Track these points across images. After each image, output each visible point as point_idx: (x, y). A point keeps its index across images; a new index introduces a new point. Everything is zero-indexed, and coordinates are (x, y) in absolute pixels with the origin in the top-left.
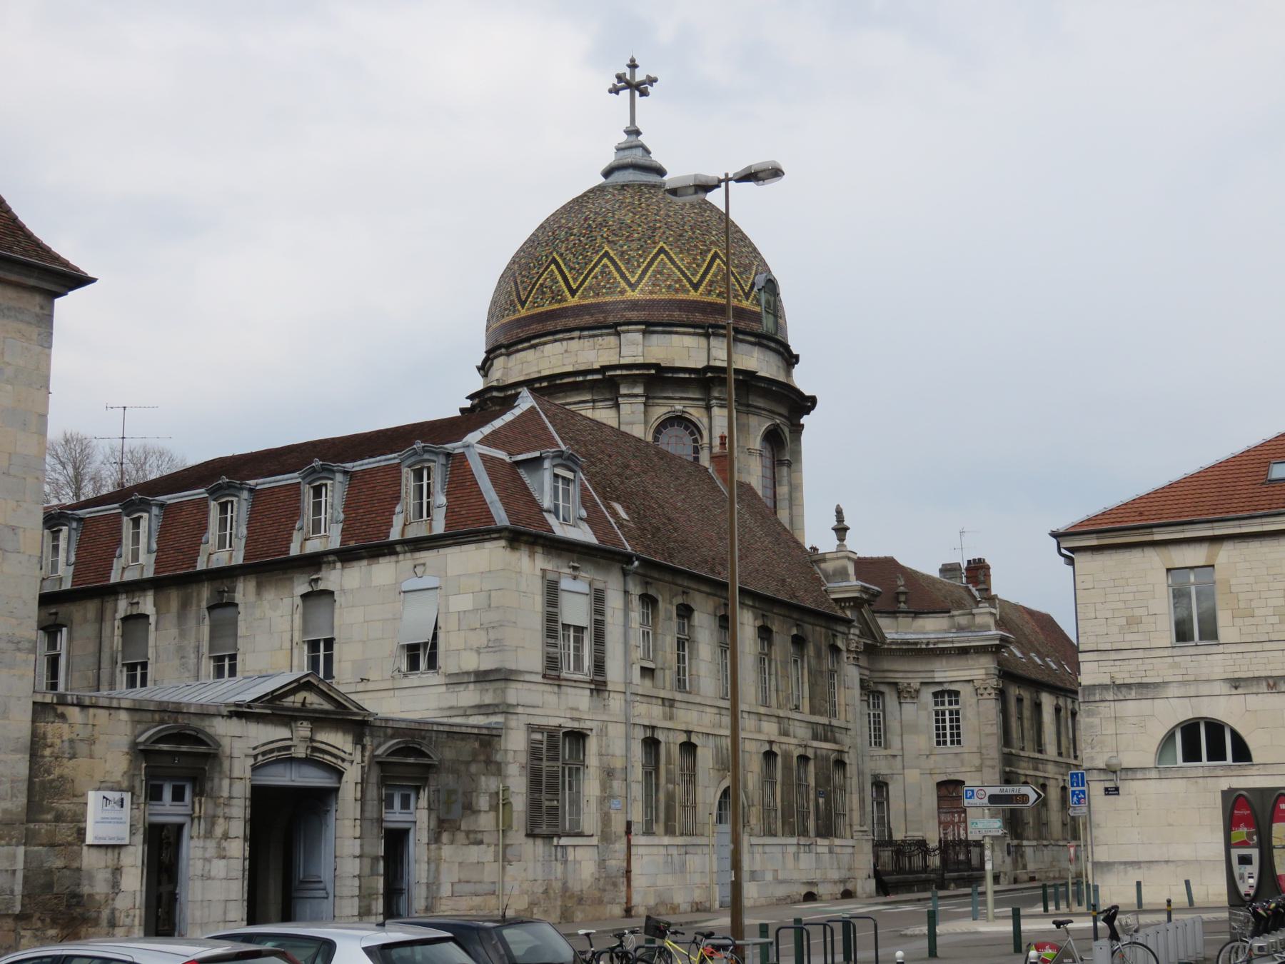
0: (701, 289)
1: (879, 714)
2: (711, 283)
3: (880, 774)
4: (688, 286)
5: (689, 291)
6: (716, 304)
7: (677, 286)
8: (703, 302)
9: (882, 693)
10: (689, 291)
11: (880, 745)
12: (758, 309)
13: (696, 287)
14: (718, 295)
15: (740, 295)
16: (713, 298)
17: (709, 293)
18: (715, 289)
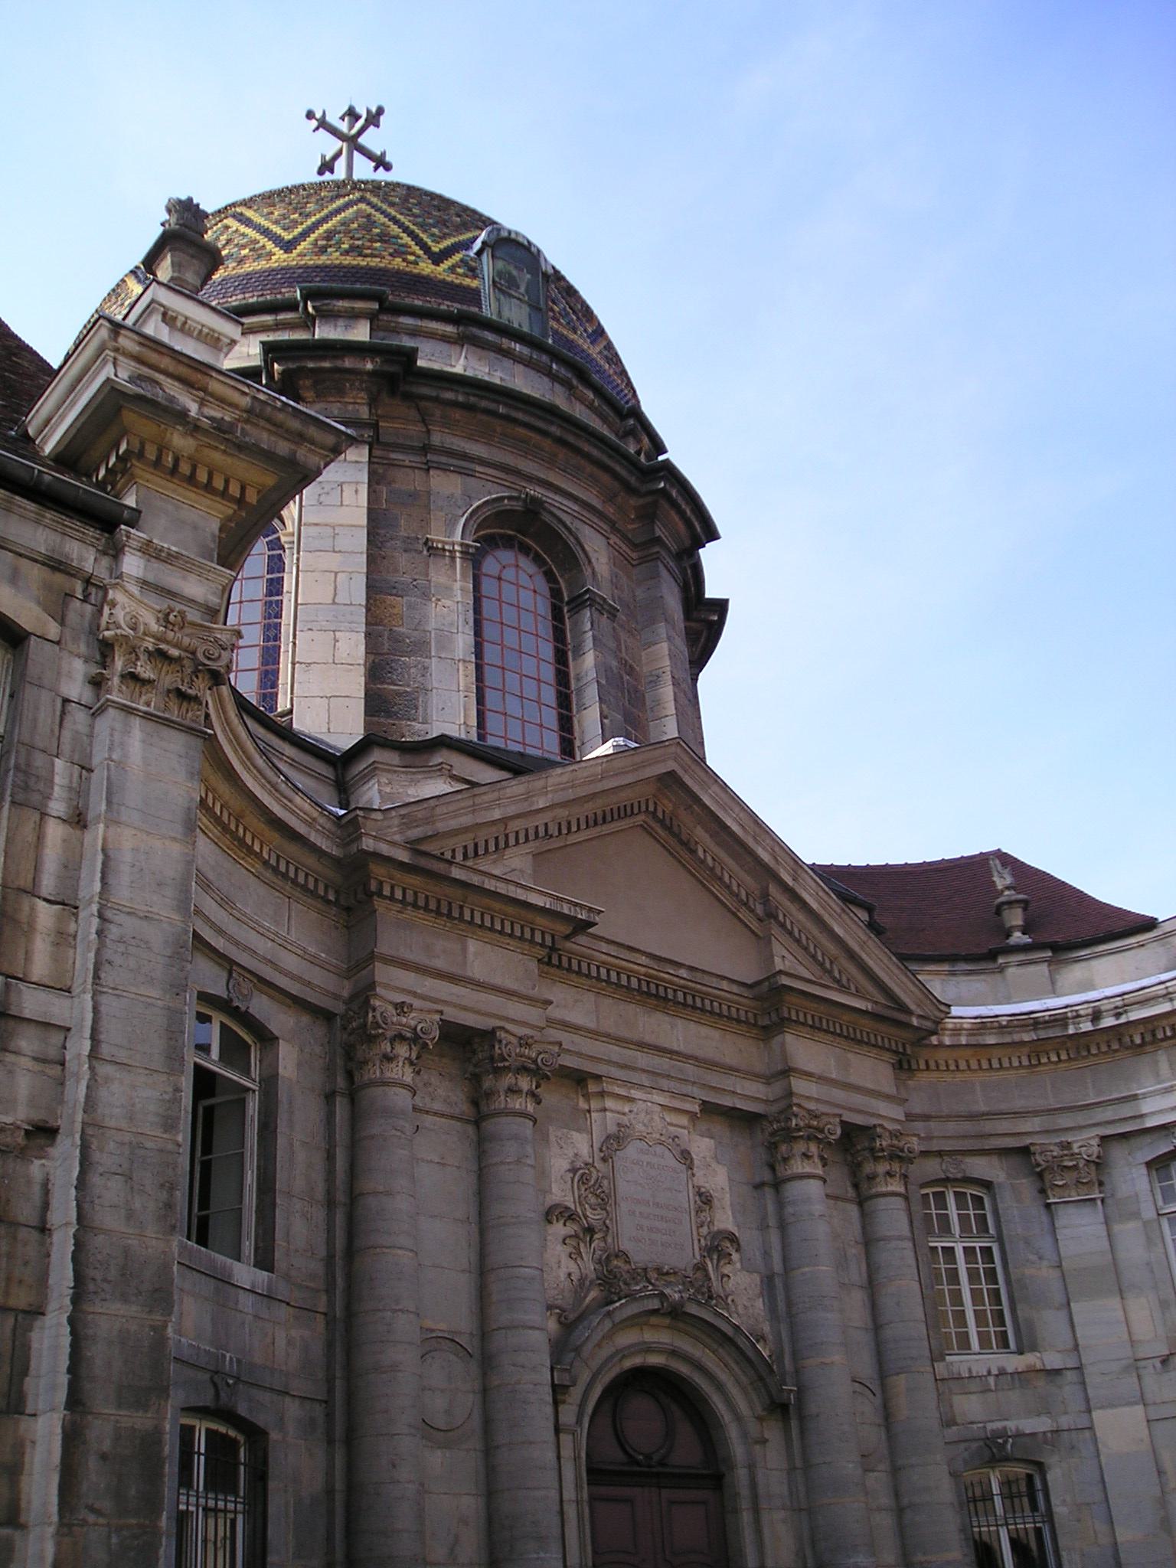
0: (303, 246)
1: (987, 1252)
2: (329, 235)
3: (1003, 1433)
4: (270, 246)
5: (271, 254)
6: (341, 267)
7: (245, 252)
8: (306, 267)
9: (987, 1185)
10: (271, 254)
11: (1004, 1342)
12: (475, 284)
13: (288, 246)
14: (346, 253)
15: (413, 254)
16: (333, 257)
17: (323, 250)
18: (339, 242)
